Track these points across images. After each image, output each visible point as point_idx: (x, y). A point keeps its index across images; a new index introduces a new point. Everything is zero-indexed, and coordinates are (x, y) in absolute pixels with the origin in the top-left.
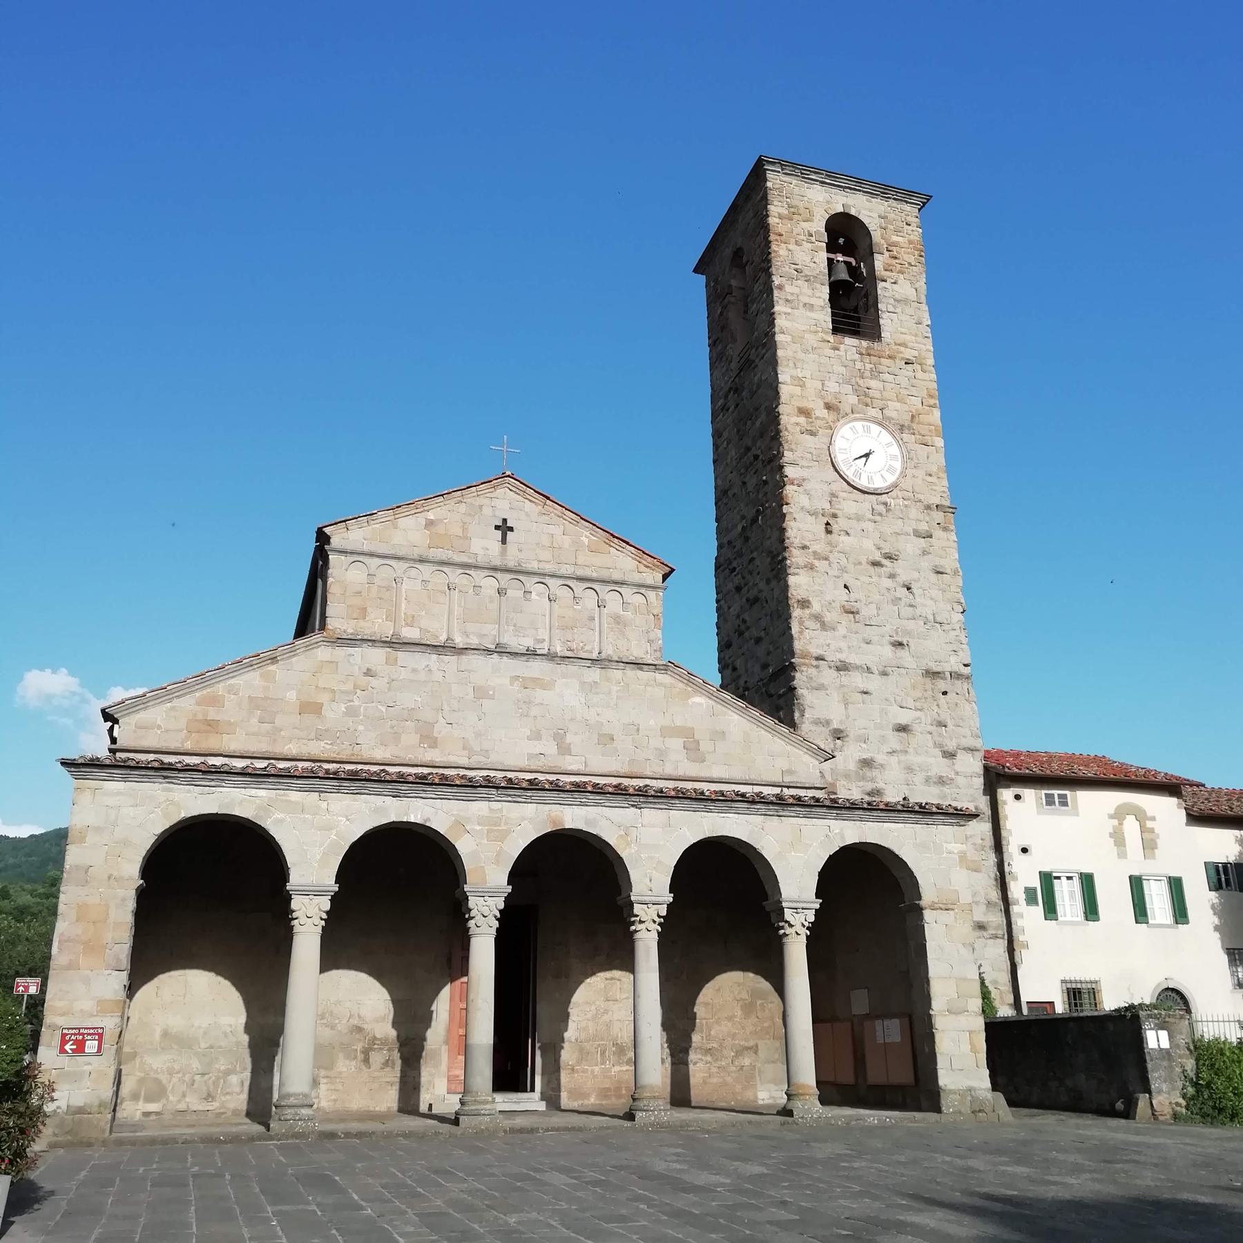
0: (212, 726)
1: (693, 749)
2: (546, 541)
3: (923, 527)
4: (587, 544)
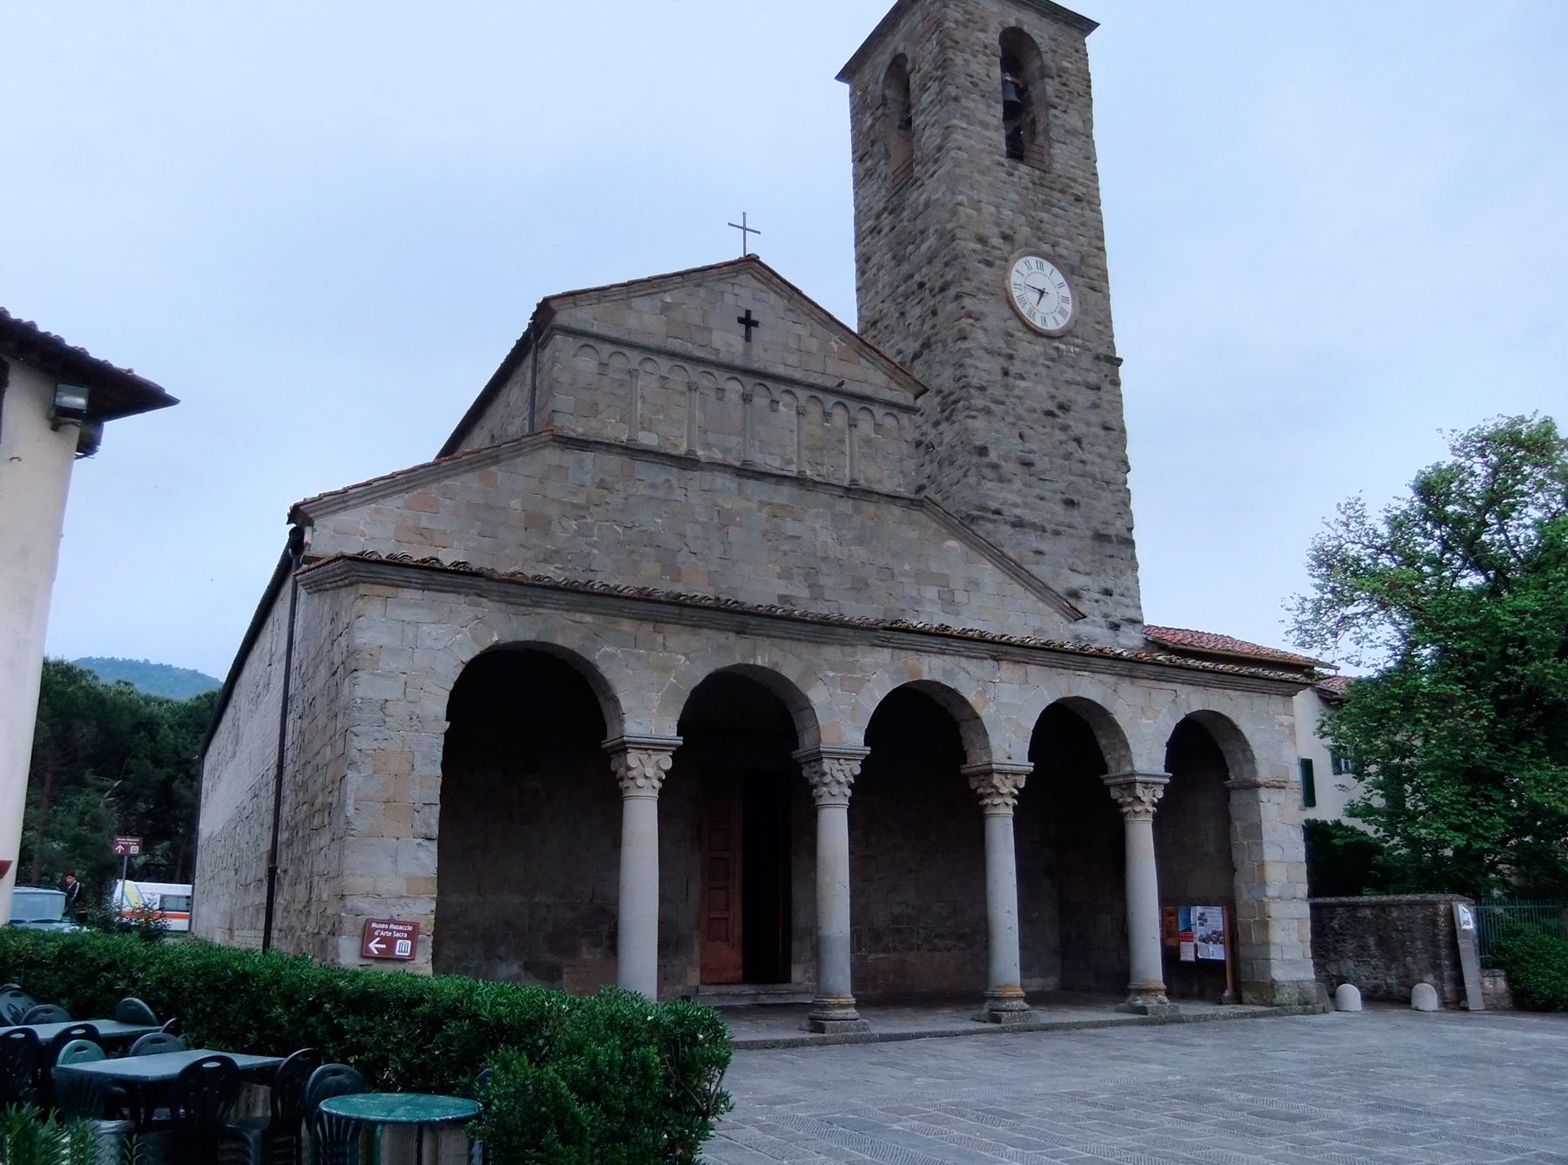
3: (1093, 378)
4: (836, 350)
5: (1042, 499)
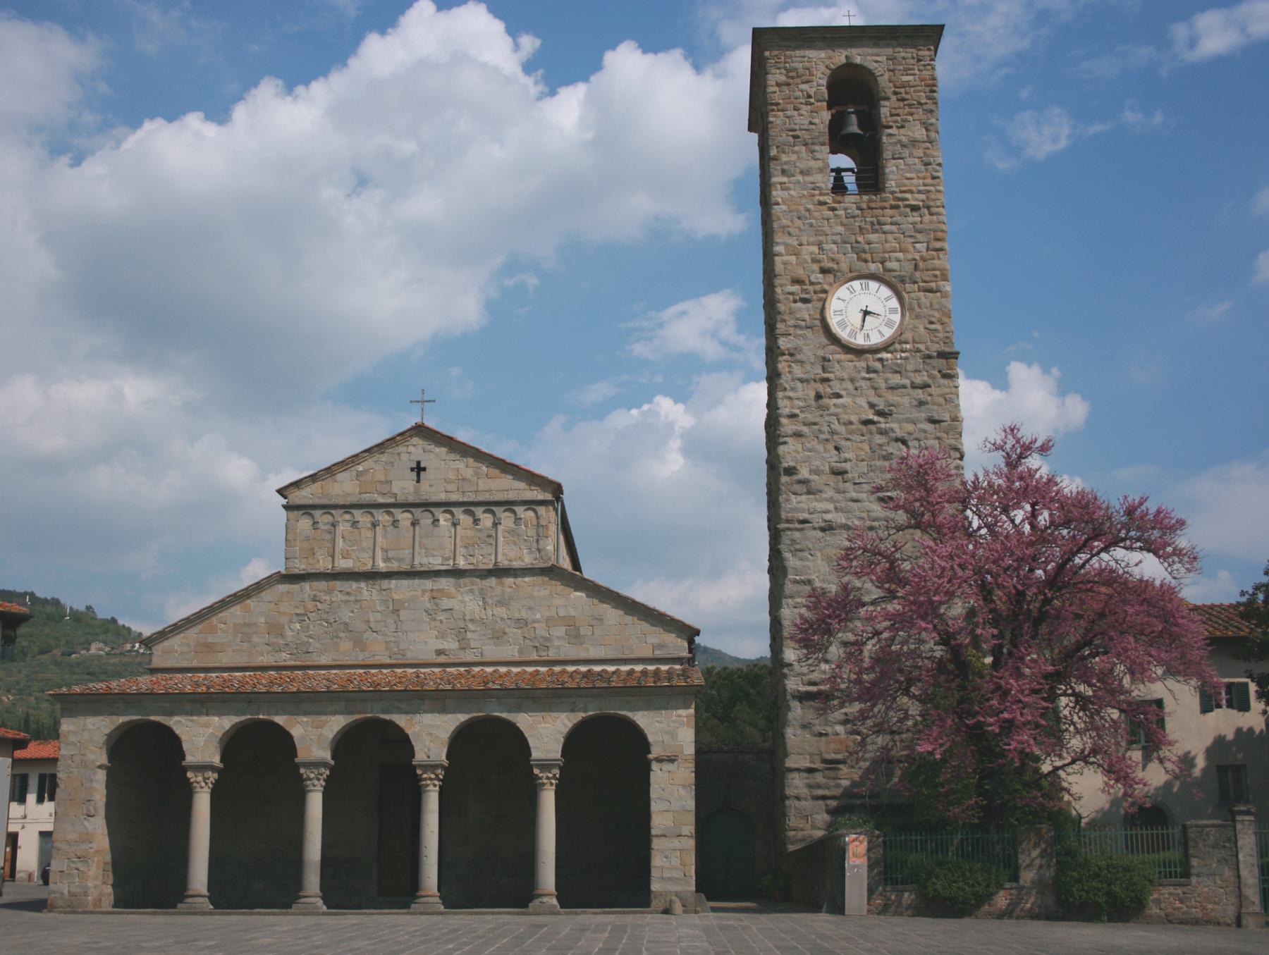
1: (574, 636)
2: (452, 476)
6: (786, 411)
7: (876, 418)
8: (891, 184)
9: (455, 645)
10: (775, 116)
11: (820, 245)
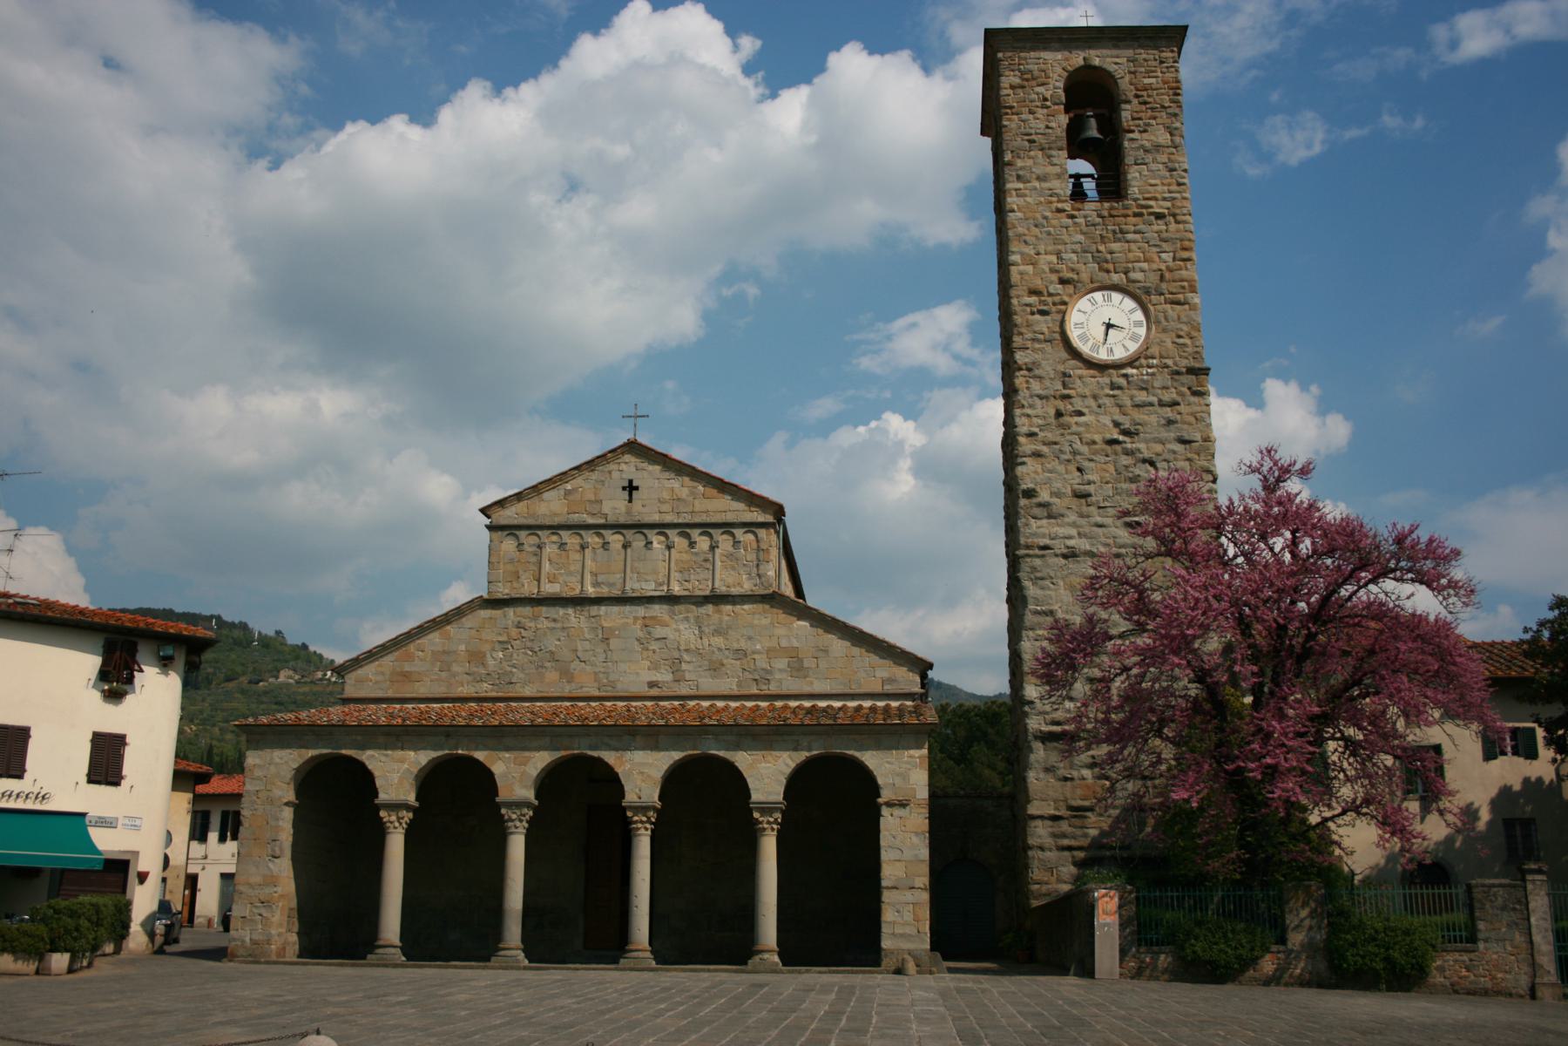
0: (406, 677)
1: (797, 668)
2: (666, 495)
5: (1101, 526)
6: (1024, 430)
7: (1121, 438)
8: (1134, 190)
9: (668, 677)
10: (1009, 120)
11: (1058, 254)
